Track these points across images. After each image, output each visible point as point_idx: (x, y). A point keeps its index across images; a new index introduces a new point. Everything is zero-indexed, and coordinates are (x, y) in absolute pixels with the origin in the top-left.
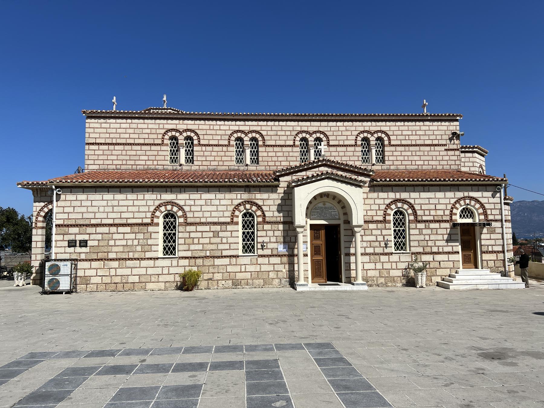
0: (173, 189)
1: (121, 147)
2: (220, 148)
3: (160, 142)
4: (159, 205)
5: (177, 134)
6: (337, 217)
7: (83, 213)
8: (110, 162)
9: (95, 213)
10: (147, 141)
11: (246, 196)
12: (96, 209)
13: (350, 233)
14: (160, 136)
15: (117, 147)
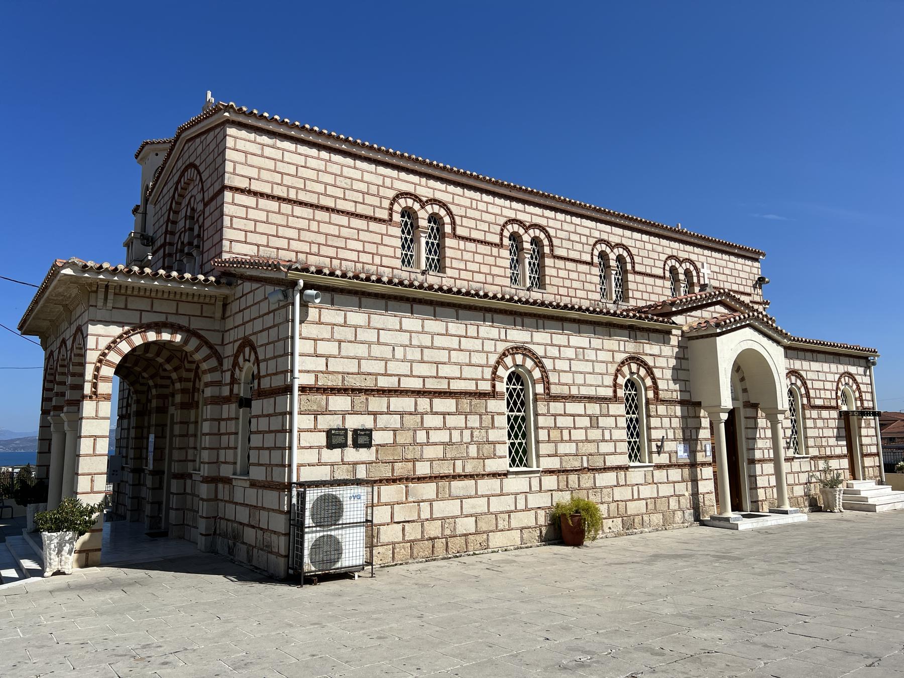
0: (527, 320)
1: (307, 212)
3: (384, 215)
4: (504, 354)
7: (360, 359)
8: (283, 243)
9: (386, 361)
10: (361, 209)
11: (631, 347)
12: (387, 352)
14: (386, 204)
15: (299, 210)
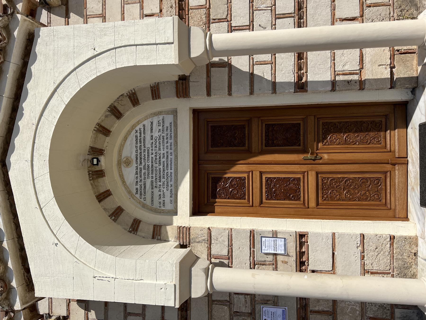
6: (169, 119)
13: (219, 76)
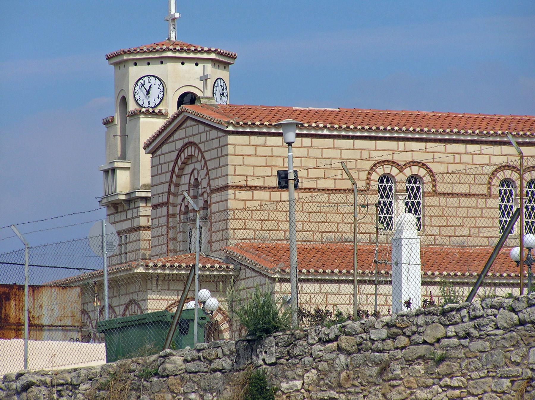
2: (472, 202)
5: (394, 171)
